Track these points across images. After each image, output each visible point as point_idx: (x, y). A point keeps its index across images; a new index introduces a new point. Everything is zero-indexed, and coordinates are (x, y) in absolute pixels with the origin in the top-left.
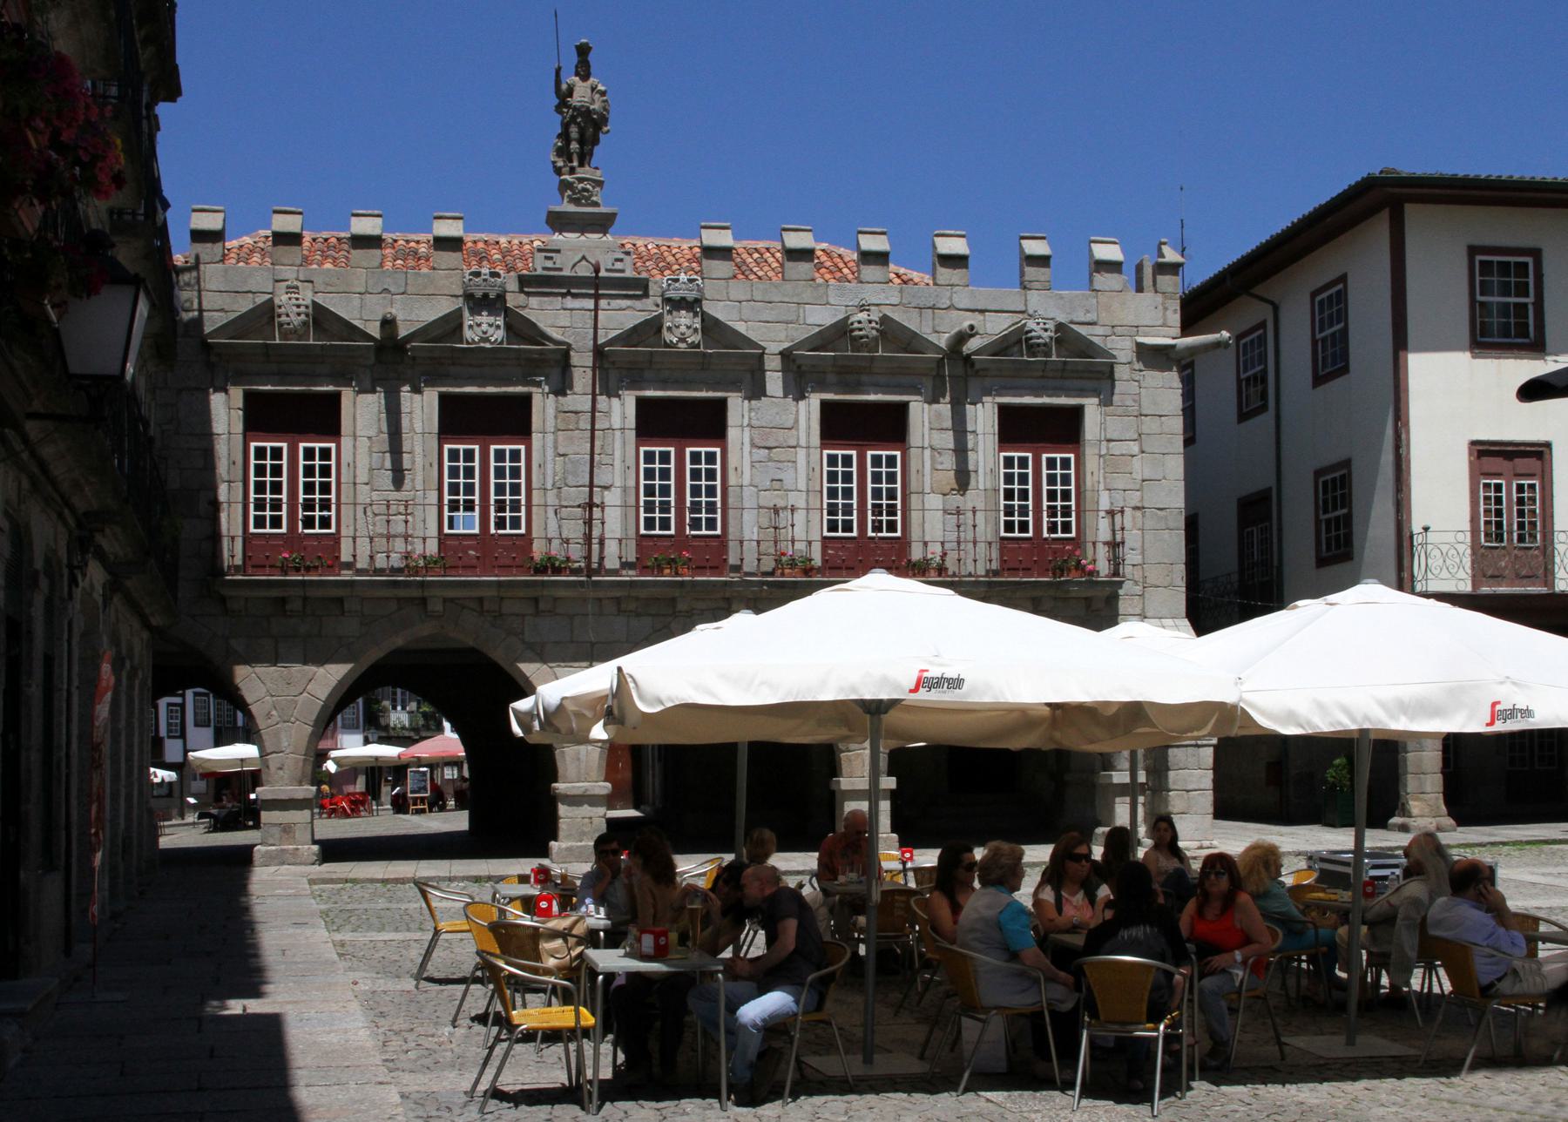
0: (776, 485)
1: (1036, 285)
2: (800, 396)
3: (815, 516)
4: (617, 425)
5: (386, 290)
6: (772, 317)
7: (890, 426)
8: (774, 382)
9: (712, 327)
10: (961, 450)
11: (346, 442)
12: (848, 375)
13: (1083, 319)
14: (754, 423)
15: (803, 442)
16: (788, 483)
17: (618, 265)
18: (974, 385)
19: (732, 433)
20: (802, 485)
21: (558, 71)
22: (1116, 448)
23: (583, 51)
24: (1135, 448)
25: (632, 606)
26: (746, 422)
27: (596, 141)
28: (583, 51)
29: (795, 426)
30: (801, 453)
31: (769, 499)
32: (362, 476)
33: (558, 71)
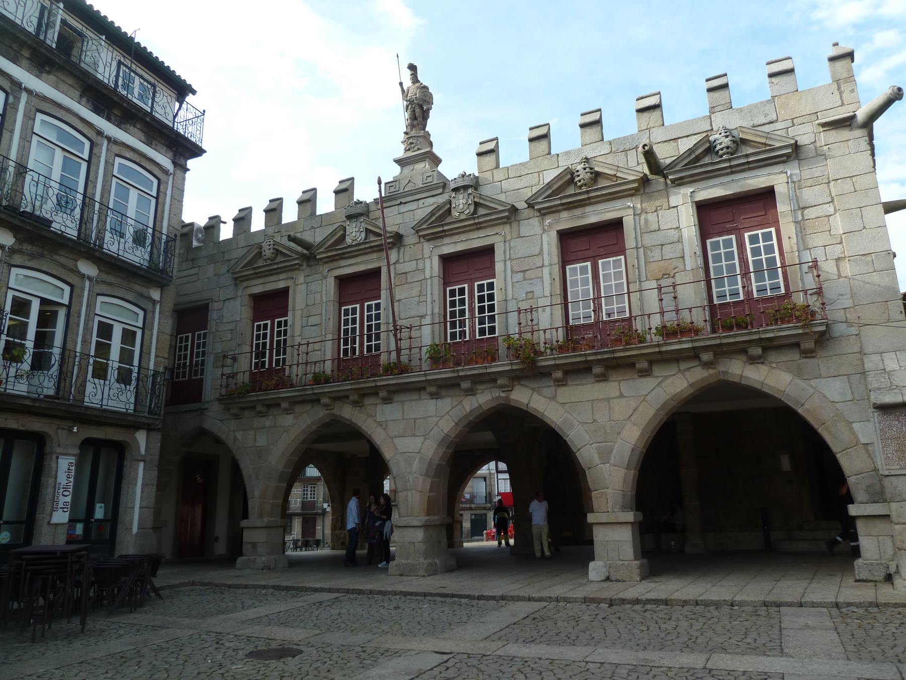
0: (530, 295)
1: (720, 108)
4: (428, 277)
5: (313, 227)
13: (765, 121)
14: (513, 256)
15: (546, 263)
16: (538, 293)
17: (430, 179)
19: (499, 267)
20: (547, 293)
21: (401, 84)
22: (810, 213)
23: (413, 68)
24: (830, 209)
25: (433, 389)
26: (508, 257)
29: (541, 253)
31: (524, 305)
32: (297, 331)
33: (401, 84)
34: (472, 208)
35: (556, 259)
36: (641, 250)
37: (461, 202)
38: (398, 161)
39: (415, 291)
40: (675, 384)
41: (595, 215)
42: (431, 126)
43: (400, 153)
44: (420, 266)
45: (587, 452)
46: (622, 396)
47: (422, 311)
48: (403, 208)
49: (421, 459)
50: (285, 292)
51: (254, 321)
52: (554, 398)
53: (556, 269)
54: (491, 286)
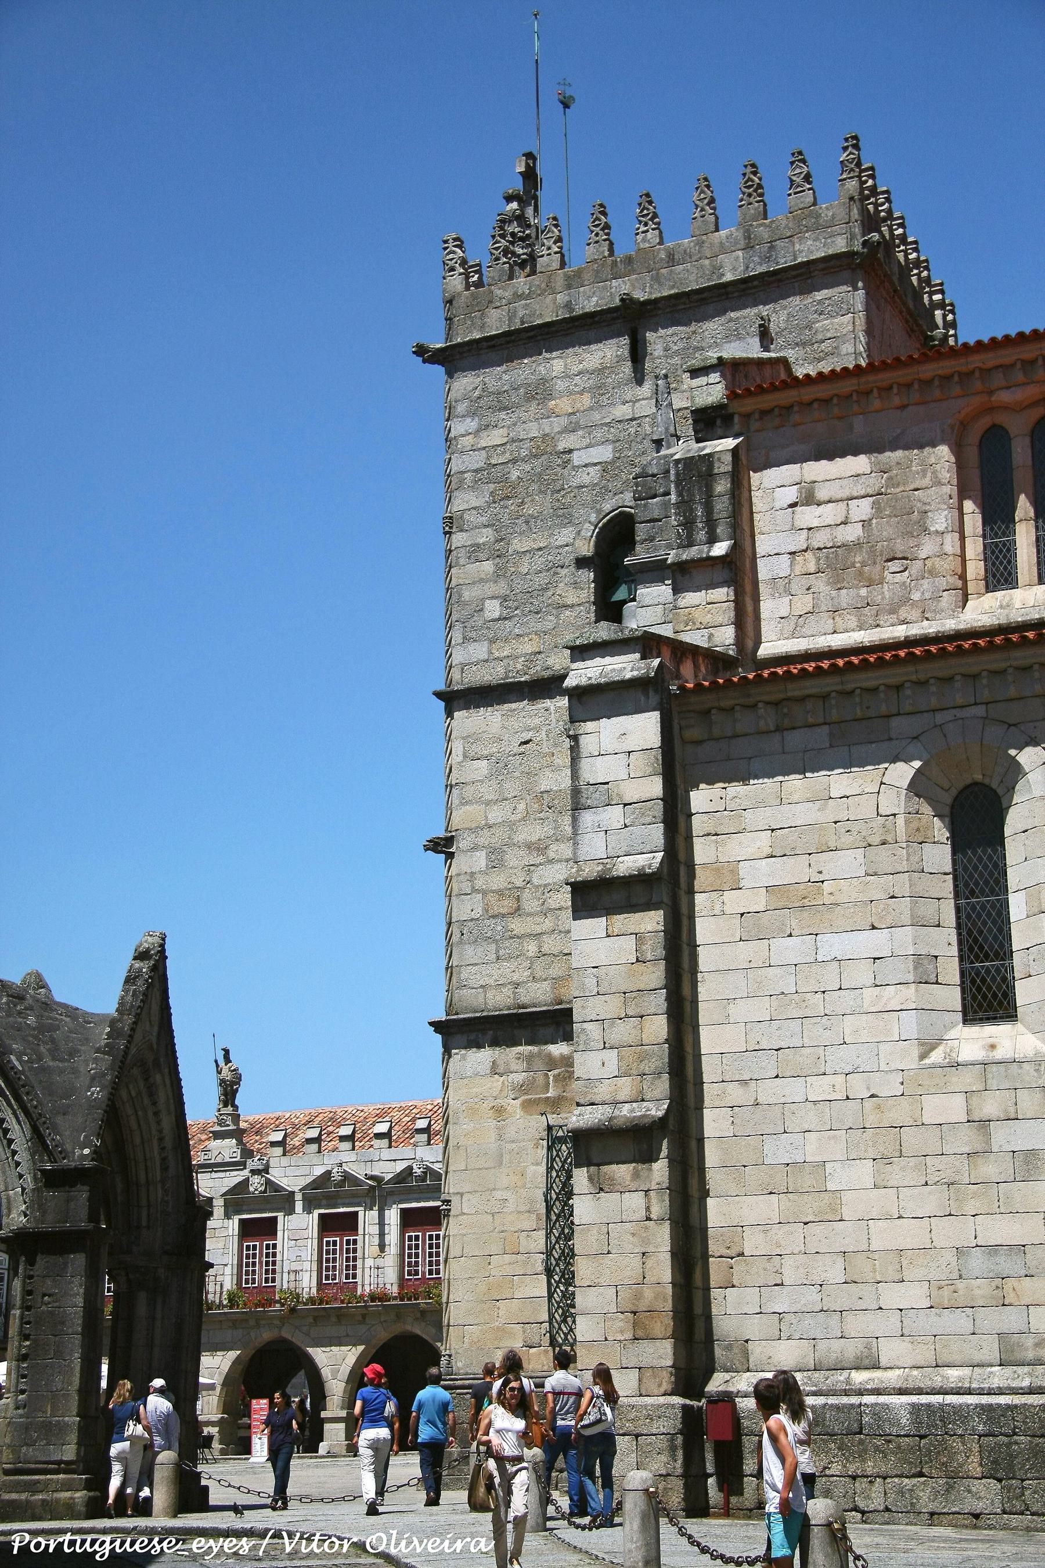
2: (309, 1213)
3: (315, 1274)
6: (291, 1174)
7: (348, 1224)
8: (299, 1206)
9: (268, 1182)
10: (382, 1235)
12: (332, 1200)
17: (235, 1155)
18: (389, 1200)
19: (280, 1234)
30: (310, 1241)
31: (295, 1266)
33: (216, 1061)
34: (263, 1188)
35: (316, 1235)
36: (367, 1237)
37: (256, 1184)
39: (221, 1245)
44: (226, 1225)
45: (326, 1373)
46: (347, 1335)
48: (214, 1175)
49: (220, 1373)
53: (315, 1242)
54: (275, 1246)
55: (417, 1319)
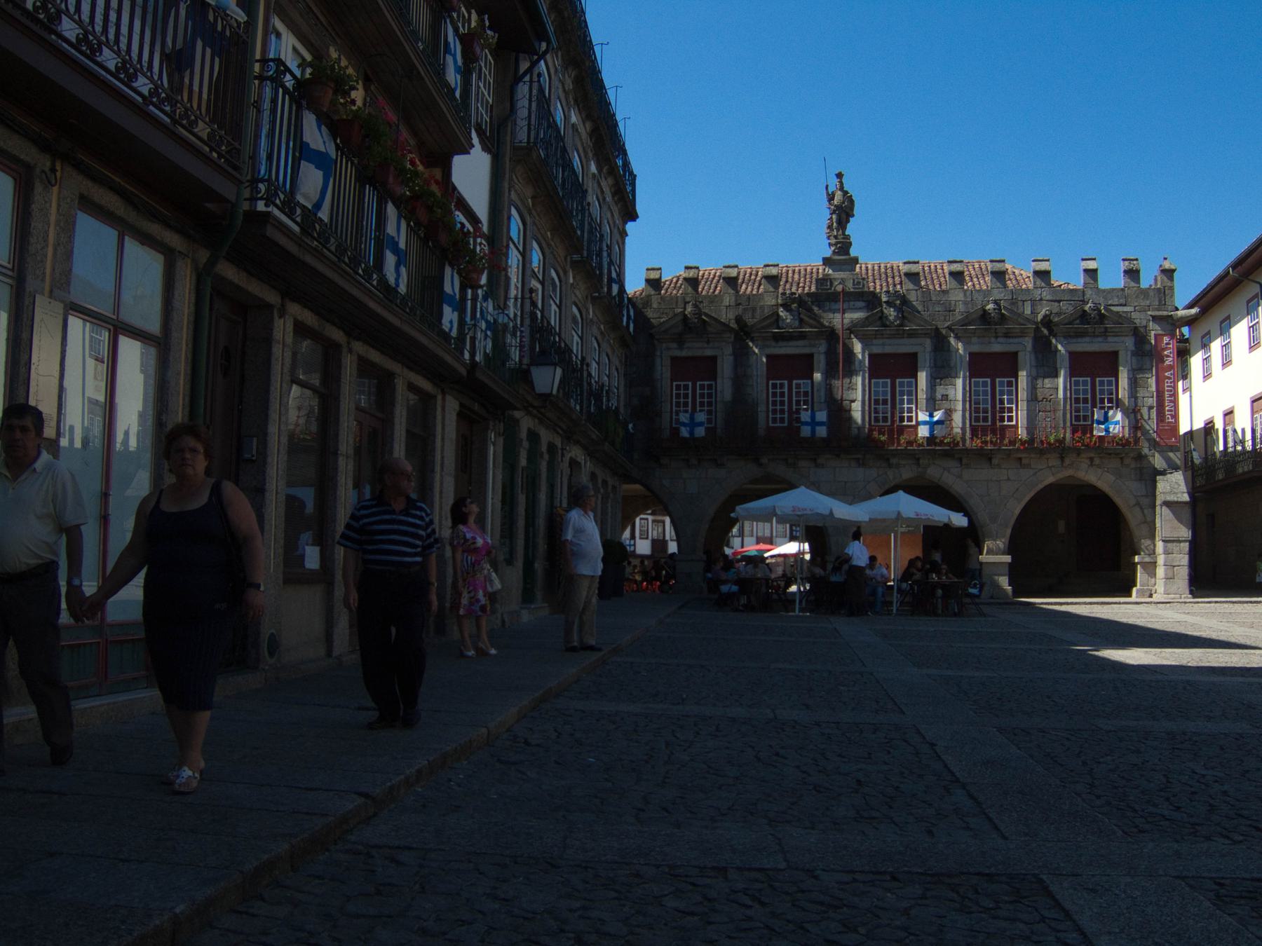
11: (719, 381)
16: (951, 397)
23: (839, 176)
27: (848, 221)
28: (839, 176)
38: (827, 261)
40: (1048, 475)
41: (997, 347)
42: (851, 229)
43: (828, 252)
47: (852, 397)
50: (713, 359)
51: (672, 381)
52: (960, 477)
55: (1091, 465)
